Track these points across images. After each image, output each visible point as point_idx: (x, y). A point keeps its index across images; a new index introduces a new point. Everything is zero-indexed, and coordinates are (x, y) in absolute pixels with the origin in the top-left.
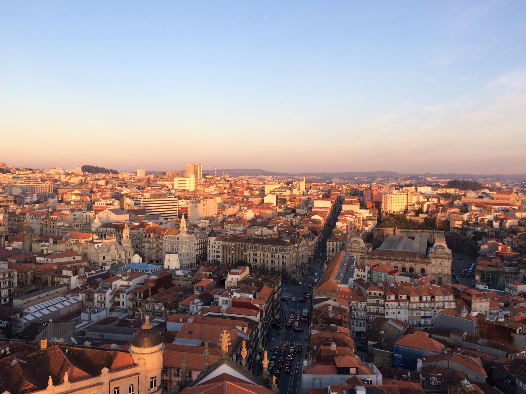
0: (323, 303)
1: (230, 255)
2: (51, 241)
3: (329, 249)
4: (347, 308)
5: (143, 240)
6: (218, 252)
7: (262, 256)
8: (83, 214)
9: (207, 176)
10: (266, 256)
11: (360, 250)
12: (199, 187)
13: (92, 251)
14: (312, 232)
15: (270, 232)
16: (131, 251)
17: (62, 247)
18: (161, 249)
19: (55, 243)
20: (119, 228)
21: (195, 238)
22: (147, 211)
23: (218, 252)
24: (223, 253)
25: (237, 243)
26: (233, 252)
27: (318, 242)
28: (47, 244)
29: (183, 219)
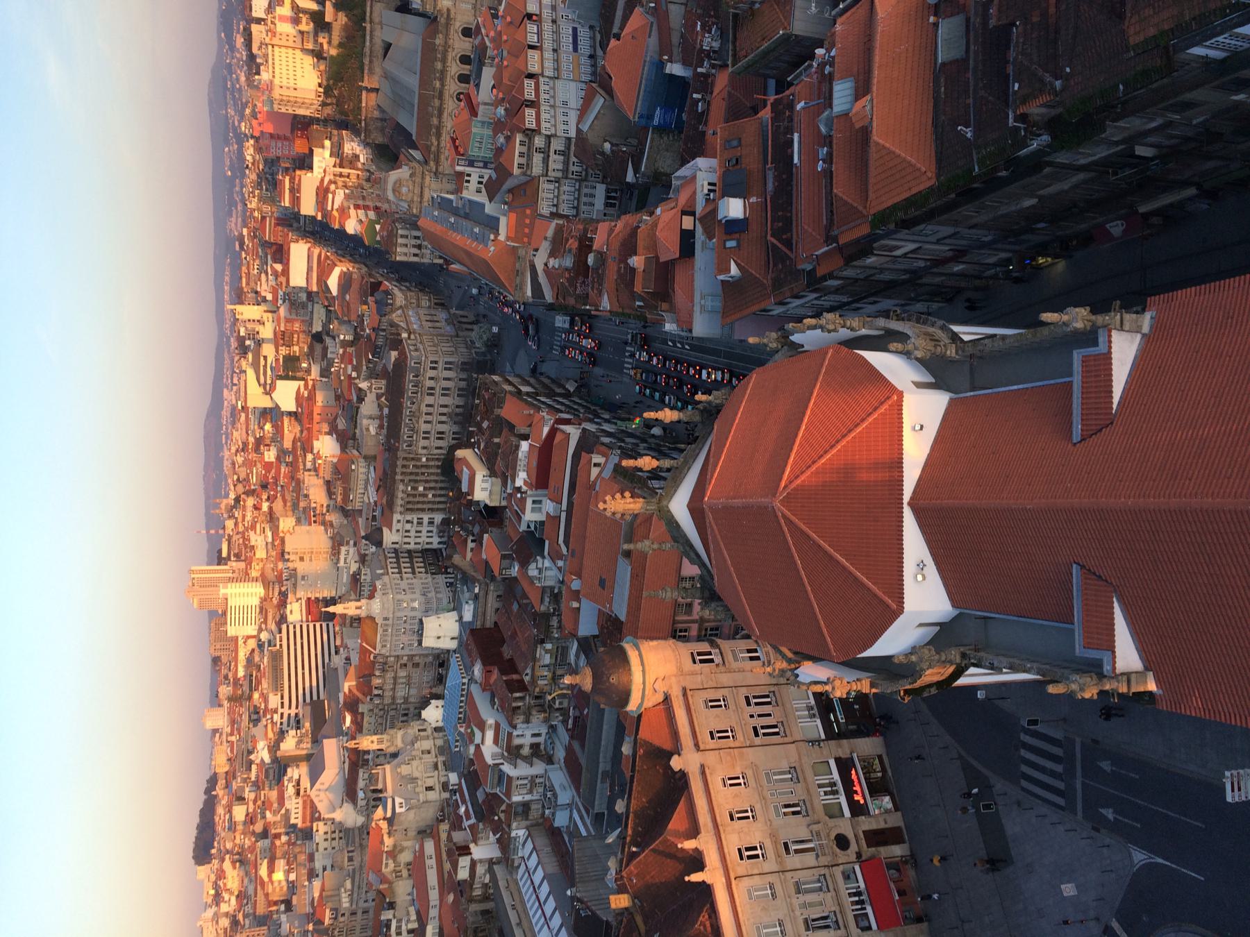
1: (426, 496)
2: (387, 915)
3: (415, 255)
4: (553, 225)
5: (387, 701)
6: (420, 523)
7: (429, 418)
8: (321, 848)
9: (224, 554)
11: (418, 180)
12: (254, 574)
13: (411, 819)
14: (372, 295)
15: (370, 398)
16: (414, 727)
17: (403, 890)
18: (411, 657)
19: (392, 906)
20: (357, 761)
21: (386, 578)
22: (315, 698)
23: (420, 523)
24: (423, 510)
25: (398, 477)
26: (421, 489)
27: (397, 281)
29: (337, 609)
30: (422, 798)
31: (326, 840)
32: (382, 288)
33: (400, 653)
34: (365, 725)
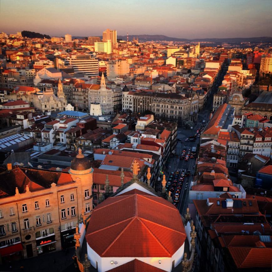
0: (208, 143)
1: (139, 105)
2: (5, 92)
3: (215, 102)
5: (74, 93)
6: (130, 103)
7: (164, 107)
8: (27, 72)
9: (120, 41)
10: (166, 107)
12: (114, 51)
13: (36, 100)
14: (203, 89)
15: (170, 88)
16: (66, 102)
17: (14, 98)
18: (87, 100)
19: (8, 94)
20: (55, 83)
21: (113, 93)
22: (75, 70)
23: (130, 103)
24: (134, 104)
25: (145, 97)
26: (141, 104)
27: (207, 96)
28: (2, 95)
30: (43, 104)
31: (29, 73)
32: (205, 92)
33: (89, 97)
34: (66, 86)
